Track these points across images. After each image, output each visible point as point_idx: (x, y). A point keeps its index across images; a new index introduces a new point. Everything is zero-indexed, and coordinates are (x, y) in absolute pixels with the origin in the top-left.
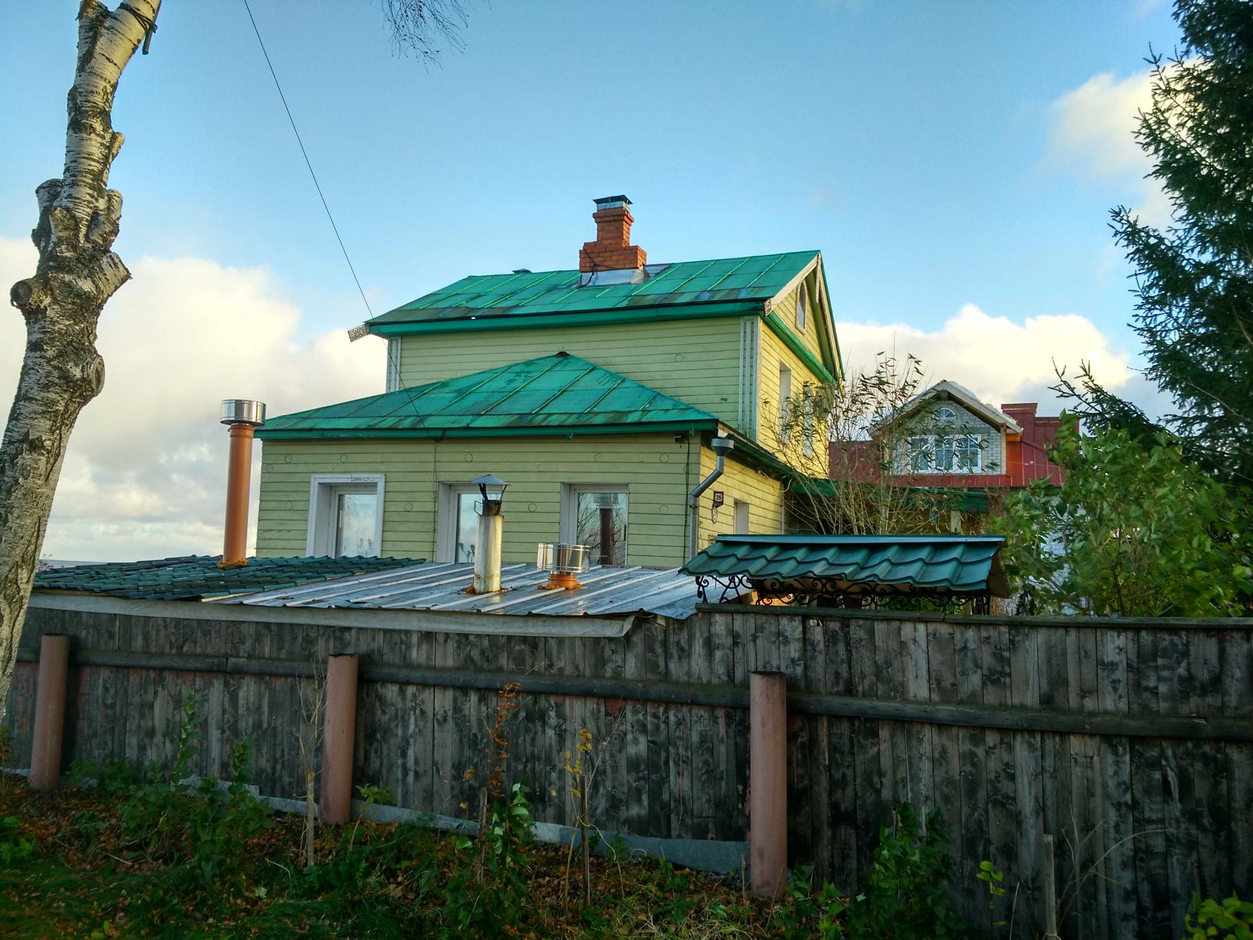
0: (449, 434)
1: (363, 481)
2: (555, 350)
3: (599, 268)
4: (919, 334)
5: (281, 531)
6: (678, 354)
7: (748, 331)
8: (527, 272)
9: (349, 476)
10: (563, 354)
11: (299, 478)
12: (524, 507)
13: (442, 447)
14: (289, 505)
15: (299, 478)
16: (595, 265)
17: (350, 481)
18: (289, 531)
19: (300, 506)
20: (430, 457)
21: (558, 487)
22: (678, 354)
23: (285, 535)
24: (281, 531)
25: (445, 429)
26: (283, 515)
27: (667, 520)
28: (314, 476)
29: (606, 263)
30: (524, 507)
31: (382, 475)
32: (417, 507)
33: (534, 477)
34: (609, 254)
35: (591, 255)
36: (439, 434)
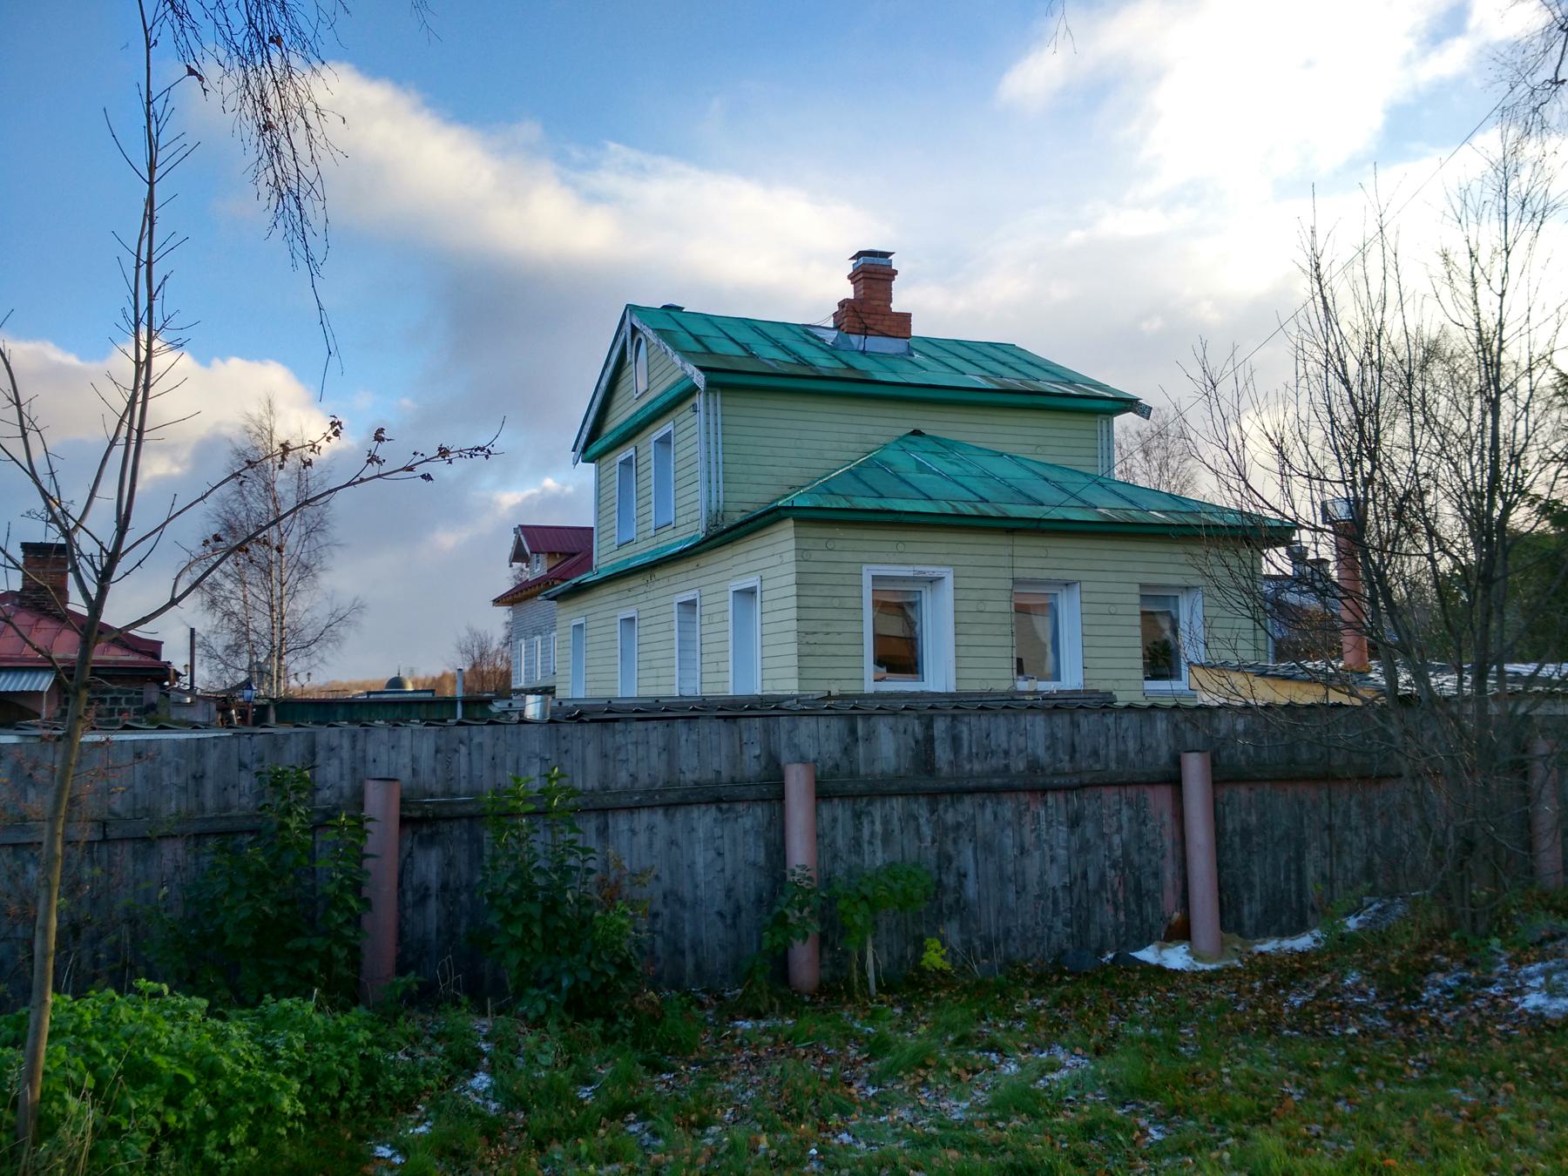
0: (1044, 525)
1: (927, 575)
2: (910, 426)
3: (869, 332)
4: (71, 360)
5: (828, 633)
6: (1039, 446)
7: (1105, 430)
8: (680, 309)
9: (911, 568)
10: (916, 433)
11: (846, 568)
12: (1104, 609)
13: (1019, 541)
14: (836, 602)
15: (846, 568)
16: (867, 328)
17: (911, 574)
18: (839, 633)
19: (851, 603)
20: (1008, 551)
21: (1136, 589)
22: (1039, 446)
23: (837, 639)
24: (828, 633)
25: (1040, 520)
26: (829, 614)
27: (1124, 620)
28: (865, 567)
29: (877, 328)
30: (1104, 609)
31: (951, 569)
32: (990, 607)
33: (1112, 577)
34: (879, 317)
35: (862, 315)
36: (1034, 525)
